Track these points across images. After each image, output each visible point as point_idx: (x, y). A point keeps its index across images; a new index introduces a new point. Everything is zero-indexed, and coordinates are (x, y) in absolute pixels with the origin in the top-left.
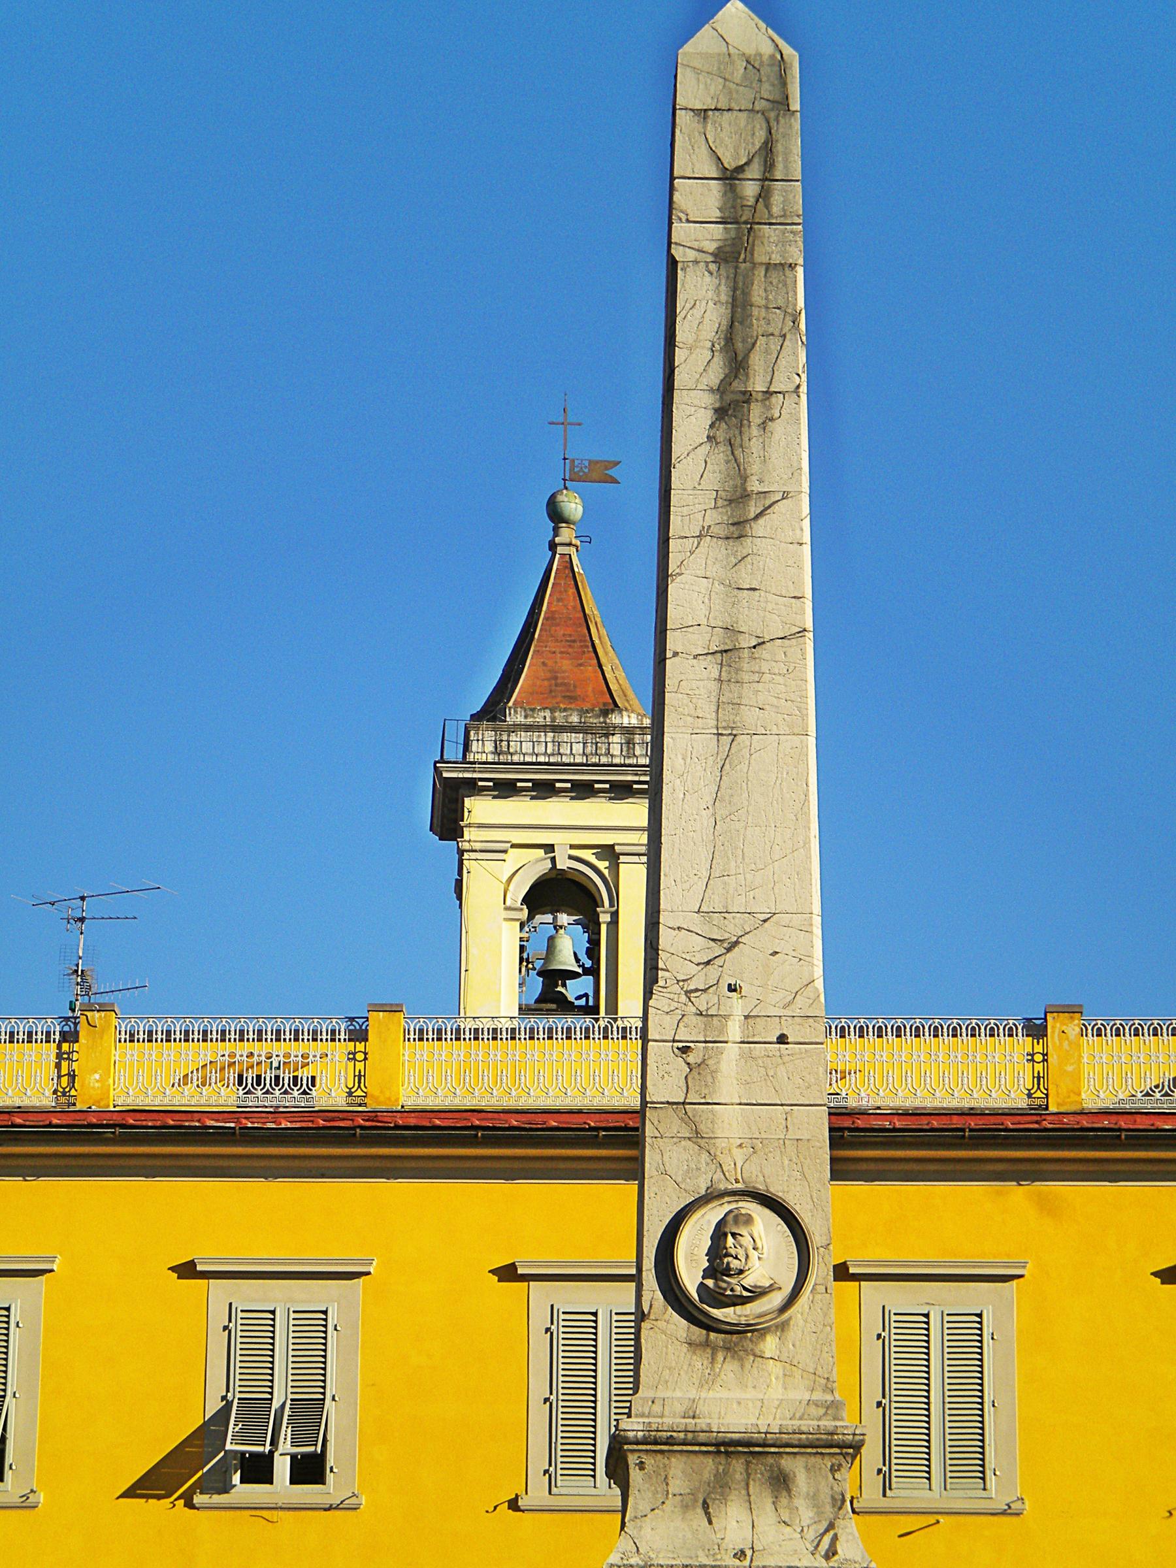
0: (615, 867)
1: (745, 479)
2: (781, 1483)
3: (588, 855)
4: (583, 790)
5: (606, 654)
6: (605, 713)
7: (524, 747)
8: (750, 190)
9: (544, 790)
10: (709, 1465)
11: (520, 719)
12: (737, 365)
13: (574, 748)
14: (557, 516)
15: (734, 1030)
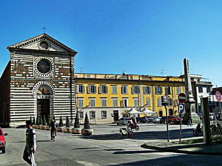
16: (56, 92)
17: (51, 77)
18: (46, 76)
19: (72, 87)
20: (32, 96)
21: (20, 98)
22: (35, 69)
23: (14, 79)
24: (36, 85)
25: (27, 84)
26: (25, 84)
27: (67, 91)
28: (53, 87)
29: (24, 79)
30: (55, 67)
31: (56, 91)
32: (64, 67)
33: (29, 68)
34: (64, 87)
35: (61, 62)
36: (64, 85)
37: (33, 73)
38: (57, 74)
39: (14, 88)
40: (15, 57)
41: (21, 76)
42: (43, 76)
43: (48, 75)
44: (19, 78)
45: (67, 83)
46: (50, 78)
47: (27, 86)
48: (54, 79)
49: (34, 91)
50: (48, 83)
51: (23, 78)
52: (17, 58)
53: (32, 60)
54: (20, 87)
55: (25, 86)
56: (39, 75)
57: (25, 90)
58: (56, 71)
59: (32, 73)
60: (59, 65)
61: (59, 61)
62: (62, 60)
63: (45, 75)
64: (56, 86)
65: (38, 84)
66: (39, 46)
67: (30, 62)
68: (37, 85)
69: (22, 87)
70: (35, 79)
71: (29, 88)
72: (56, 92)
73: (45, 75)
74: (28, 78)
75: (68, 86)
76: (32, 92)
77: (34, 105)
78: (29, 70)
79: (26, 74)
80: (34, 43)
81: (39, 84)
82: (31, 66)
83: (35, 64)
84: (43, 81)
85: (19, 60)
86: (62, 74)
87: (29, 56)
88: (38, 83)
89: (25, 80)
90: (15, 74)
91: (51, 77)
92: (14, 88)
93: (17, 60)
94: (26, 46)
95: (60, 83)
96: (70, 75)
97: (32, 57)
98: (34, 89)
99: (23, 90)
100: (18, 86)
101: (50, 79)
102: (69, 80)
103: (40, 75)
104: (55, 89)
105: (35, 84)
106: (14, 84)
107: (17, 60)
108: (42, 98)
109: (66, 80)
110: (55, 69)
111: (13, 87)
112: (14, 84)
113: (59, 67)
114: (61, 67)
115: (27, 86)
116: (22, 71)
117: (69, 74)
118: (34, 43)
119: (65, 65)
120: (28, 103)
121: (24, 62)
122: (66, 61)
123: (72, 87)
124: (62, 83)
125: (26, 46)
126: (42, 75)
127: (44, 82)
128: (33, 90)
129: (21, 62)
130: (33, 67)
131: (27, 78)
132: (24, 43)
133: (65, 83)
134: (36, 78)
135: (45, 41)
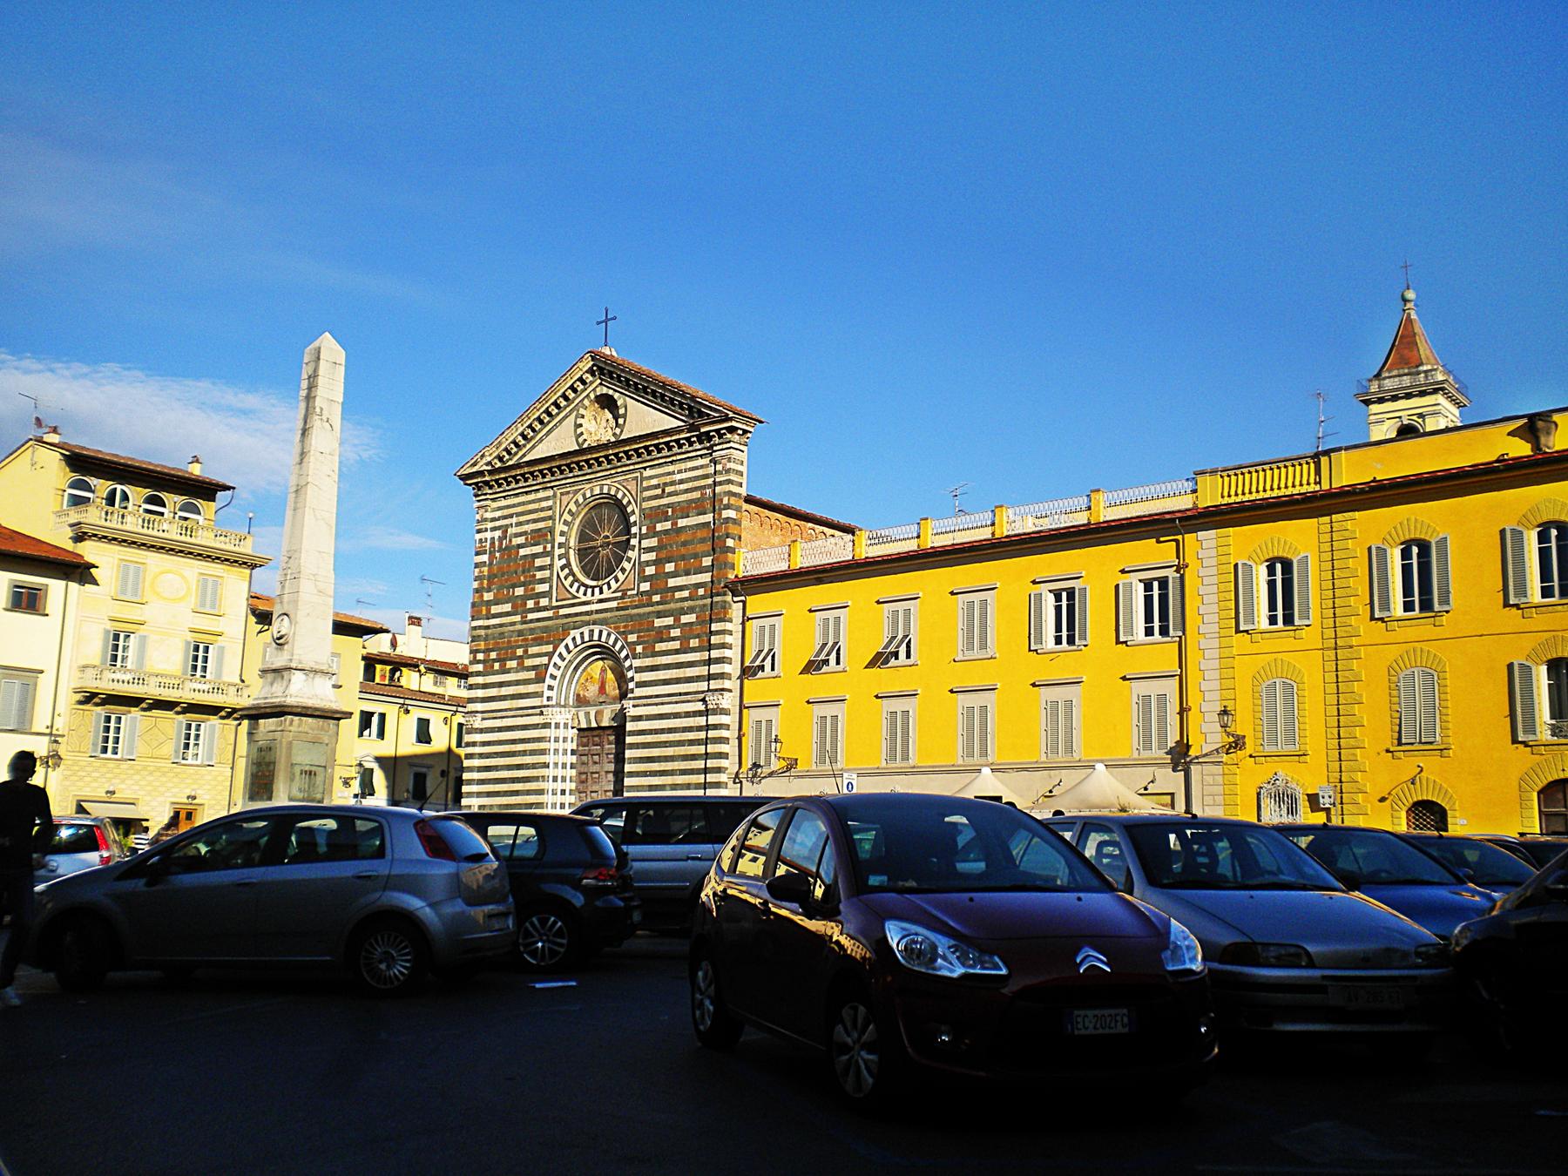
0: (1424, 421)
1: (303, 449)
2: (283, 677)
3: (1415, 418)
4: (1409, 396)
5: (1421, 342)
6: (1417, 367)
7: (1389, 384)
8: (312, 379)
9: (1395, 398)
10: (273, 674)
11: (1387, 375)
12: (305, 422)
13: (1406, 381)
14: (1405, 301)
15: (288, 577)
16: (640, 685)
17: (624, 592)
18: (601, 592)
19: (714, 640)
20: (542, 713)
21: (500, 729)
22: (564, 561)
23: (482, 632)
24: (561, 649)
25: (526, 652)
26: (520, 652)
27: (690, 672)
28: (627, 657)
29: (519, 627)
30: (640, 529)
31: (639, 677)
32: (682, 523)
33: (538, 562)
34: (676, 645)
35: (670, 494)
36: (675, 633)
37: (551, 587)
38: (650, 570)
39: (480, 680)
40: (493, 520)
41: (507, 614)
42: (589, 597)
43: (609, 588)
44: (501, 625)
45: (691, 618)
46: (614, 604)
47: (528, 662)
48: (637, 607)
49: (550, 688)
50: (609, 635)
51: (513, 624)
52: (498, 519)
53: (550, 518)
54: (504, 671)
55: (522, 668)
56: (575, 597)
57: (518, 683)
58: (645, 557)
59: (544, 587)
60: (658, 514)
61: (659, 491)
62: (673, 483)
63: (597, 590)
64: (639, 649)
65: (567, 647)
66: (579, 431)
67: (540, 529)
68: (565, 653)
69: (508, 671)
70: (558, 617)
71: (532, 674)
72: (640, 685)
73: (597, 590)
74: (531, 621)
75: (698, 636)
76: (539, 695)
77: (546, 766)
78: (539, 575)
79: (525, 598)
80: (560, 422)
81: (571, 646)
82: (544, 554)
83: (567, 533)
84: (587, 623)
85: (505, 529)
86: (670, 567)
87: (541, 500)
88: (569, 641)
89: (520, 633)
90: (489, 603)
91: (622, 598)
92: (480, 680)
93: (498, 534)
94: (528, 446)
95: (658, 623)
96: (711, 568)
97: (550, 503)
98: (553, 677)
99: (509, 684)
100: (497, 666)
101: (618, 609)
102: (703, 597)
103: (578, 591)
104: (637, 663)
105: (555, 649)
106: (480, 656)
107: (498, 534)
108: (594, 725)
109: (690, 598)
110: (640, 542)
111: (478, 674)
112: (480, 656)
113: (659, 527)
114: (668, 525)
115: (528, 662)
116: (514, 586)
117: (707, 561)
118: (560, 422)
119: (684, 510)
120: (524, 753)
121: (520, 535)
122: (690, 485)
123: (714, 640)
124: (669, 621)
125: (533, 447)
126: (585, 594)
127: (592, 631)
128: (548, 681)
129: (510, 541)
130: (550, 554)
131: (531, 616)
132: (514, 434)
133: (685, 619)
134: (562, 612)
135: (605, 390)
